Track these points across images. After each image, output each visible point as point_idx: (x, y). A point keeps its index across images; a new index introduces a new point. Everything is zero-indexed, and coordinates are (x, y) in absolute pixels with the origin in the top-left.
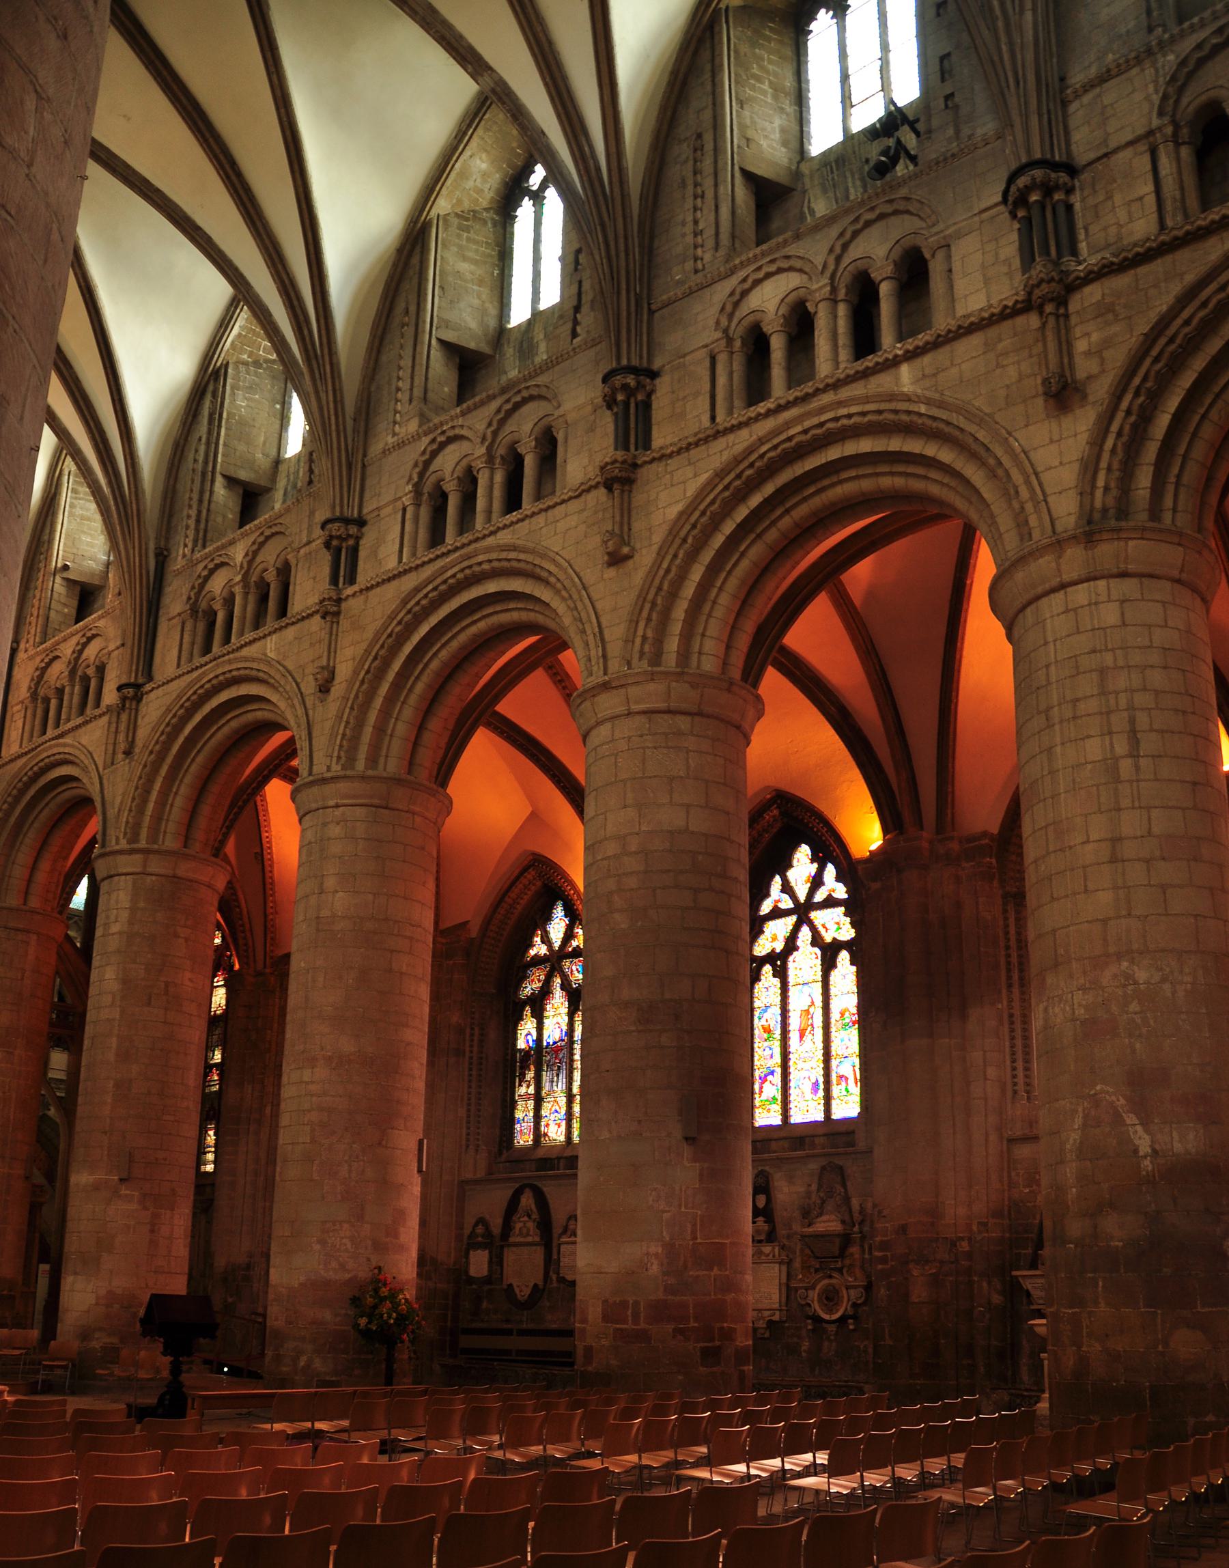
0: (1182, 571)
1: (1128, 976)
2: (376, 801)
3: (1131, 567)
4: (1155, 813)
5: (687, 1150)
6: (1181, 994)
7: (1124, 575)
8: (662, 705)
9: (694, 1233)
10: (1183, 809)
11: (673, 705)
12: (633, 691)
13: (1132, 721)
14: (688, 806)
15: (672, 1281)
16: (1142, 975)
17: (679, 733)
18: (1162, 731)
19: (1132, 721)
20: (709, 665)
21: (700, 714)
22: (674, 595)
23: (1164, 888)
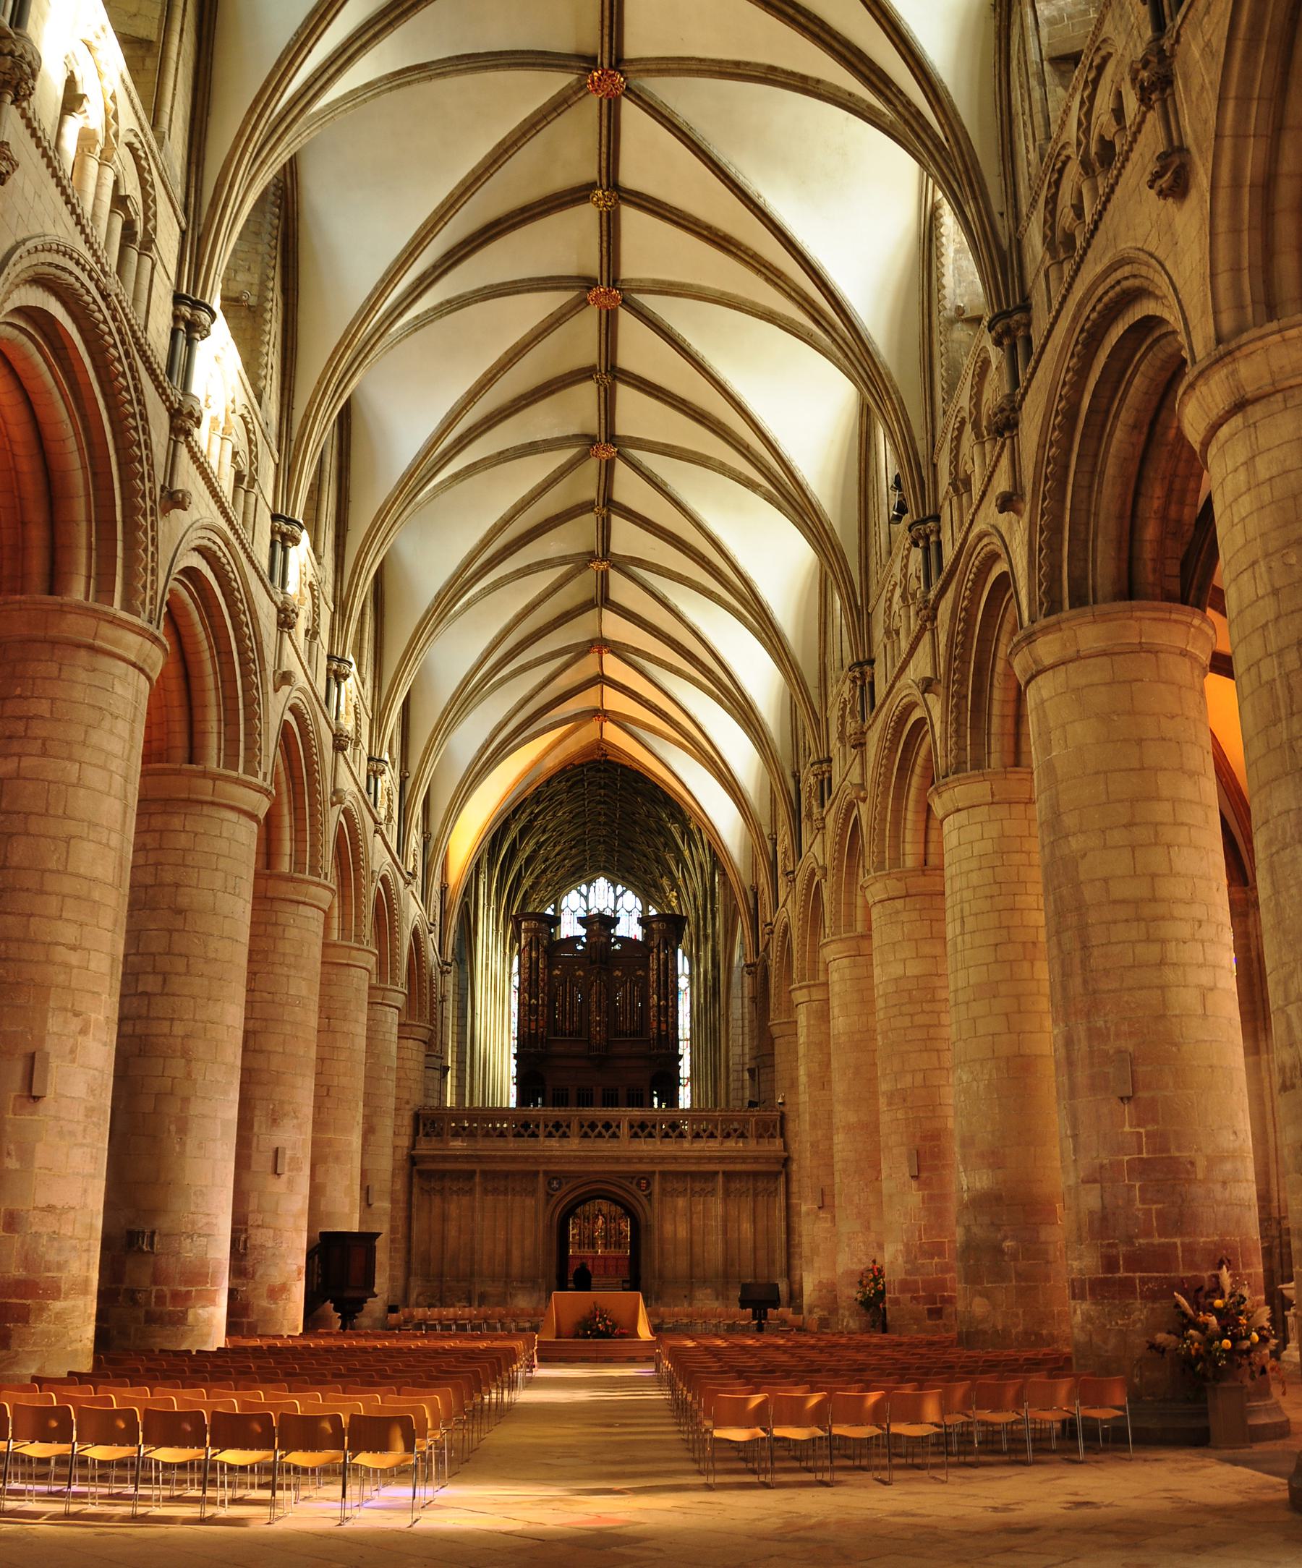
0: (993, 796)
1: (960, 1079)
2: (853, 953)
3: (961, 805)
4: (971, 970)
5: (914, 1184)
6: (982, 1087)
7: (958, 810)
8: (884, 896)
9: (920, 1236)
10: (987, 964)
11: (892, 894)
12: (871, 888)
13: (962, 910)
14: (905, 960)
15: (909, 1266)
16: (964, 1078)
17: (897, 912)
18: (976, 914)
19: (962, 910)
20: (910, 862)
21: (907, 896)
22: (883, 820)
23: (974, 1019)
